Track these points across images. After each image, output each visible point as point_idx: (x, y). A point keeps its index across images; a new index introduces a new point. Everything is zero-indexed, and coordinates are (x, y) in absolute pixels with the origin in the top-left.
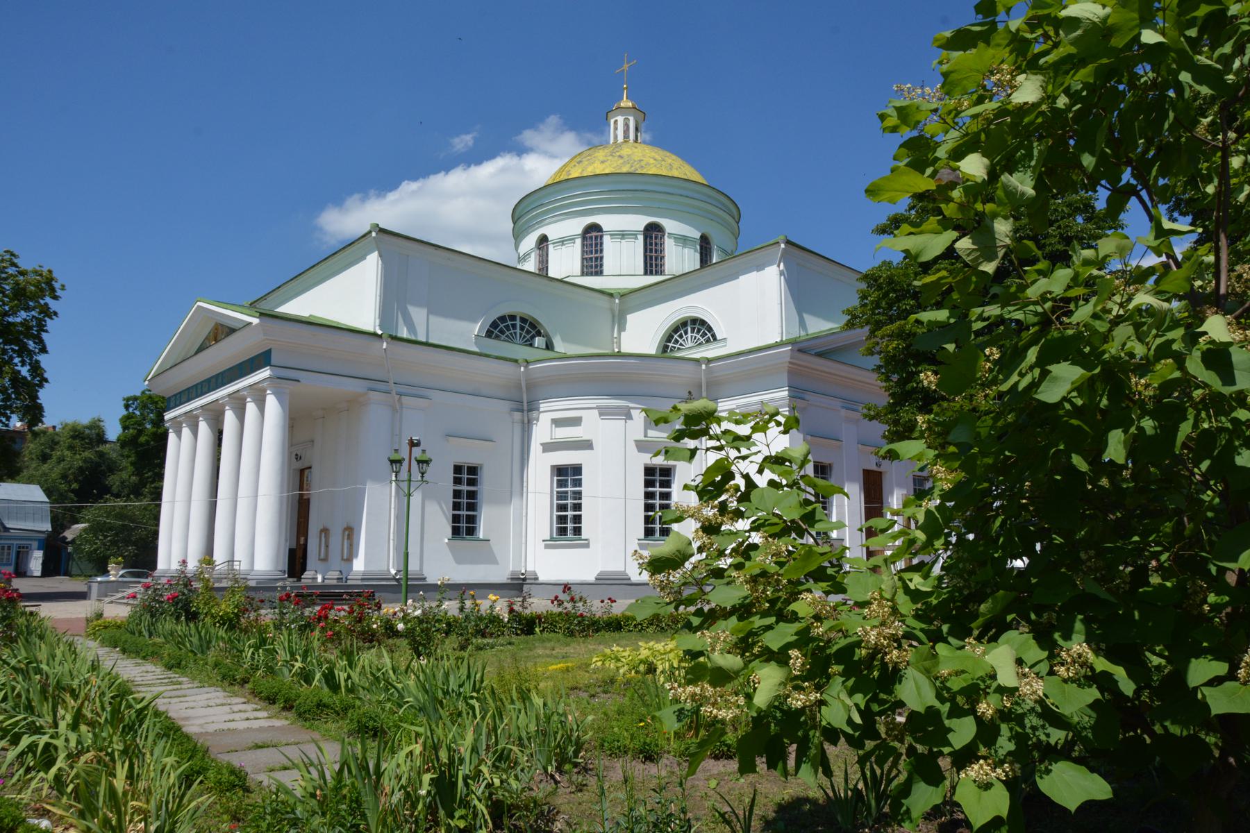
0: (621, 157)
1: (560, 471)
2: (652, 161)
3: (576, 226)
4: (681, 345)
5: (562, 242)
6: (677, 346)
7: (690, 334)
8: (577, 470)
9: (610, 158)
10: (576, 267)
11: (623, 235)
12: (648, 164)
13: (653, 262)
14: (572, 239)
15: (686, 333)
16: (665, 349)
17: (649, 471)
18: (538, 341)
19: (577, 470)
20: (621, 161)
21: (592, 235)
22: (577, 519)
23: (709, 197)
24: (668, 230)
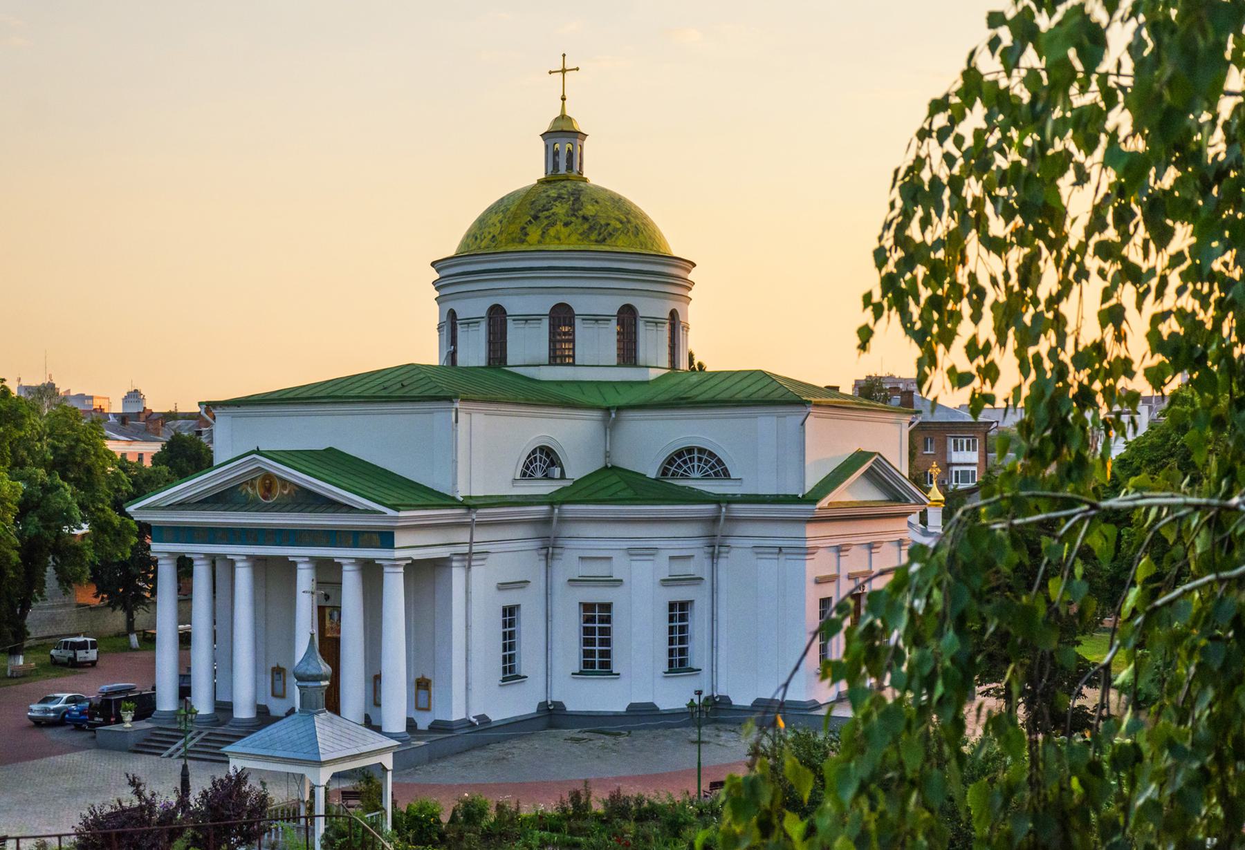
0: (585, 218)
1: (587, 607)
2: (619, 226)
3: (544, 304)
4: (685, 471)
5: (527, 319)
6: (681, 472)
7: (696, 464)
8: (607, 607)
9: (574, 219)
10: (544, 352)
11: (596, 319)
12: (616, 230)
13: (628, 355)
14: (537, 318)
15: (692, 460)
16: (664, 472)
17: (672, 606)
18: (557, 472)
19: (607, 607)
20: (586, 226)
21: (562, 317)
22: (606, 654)
23: (676, 266)
24: (641, 313)
